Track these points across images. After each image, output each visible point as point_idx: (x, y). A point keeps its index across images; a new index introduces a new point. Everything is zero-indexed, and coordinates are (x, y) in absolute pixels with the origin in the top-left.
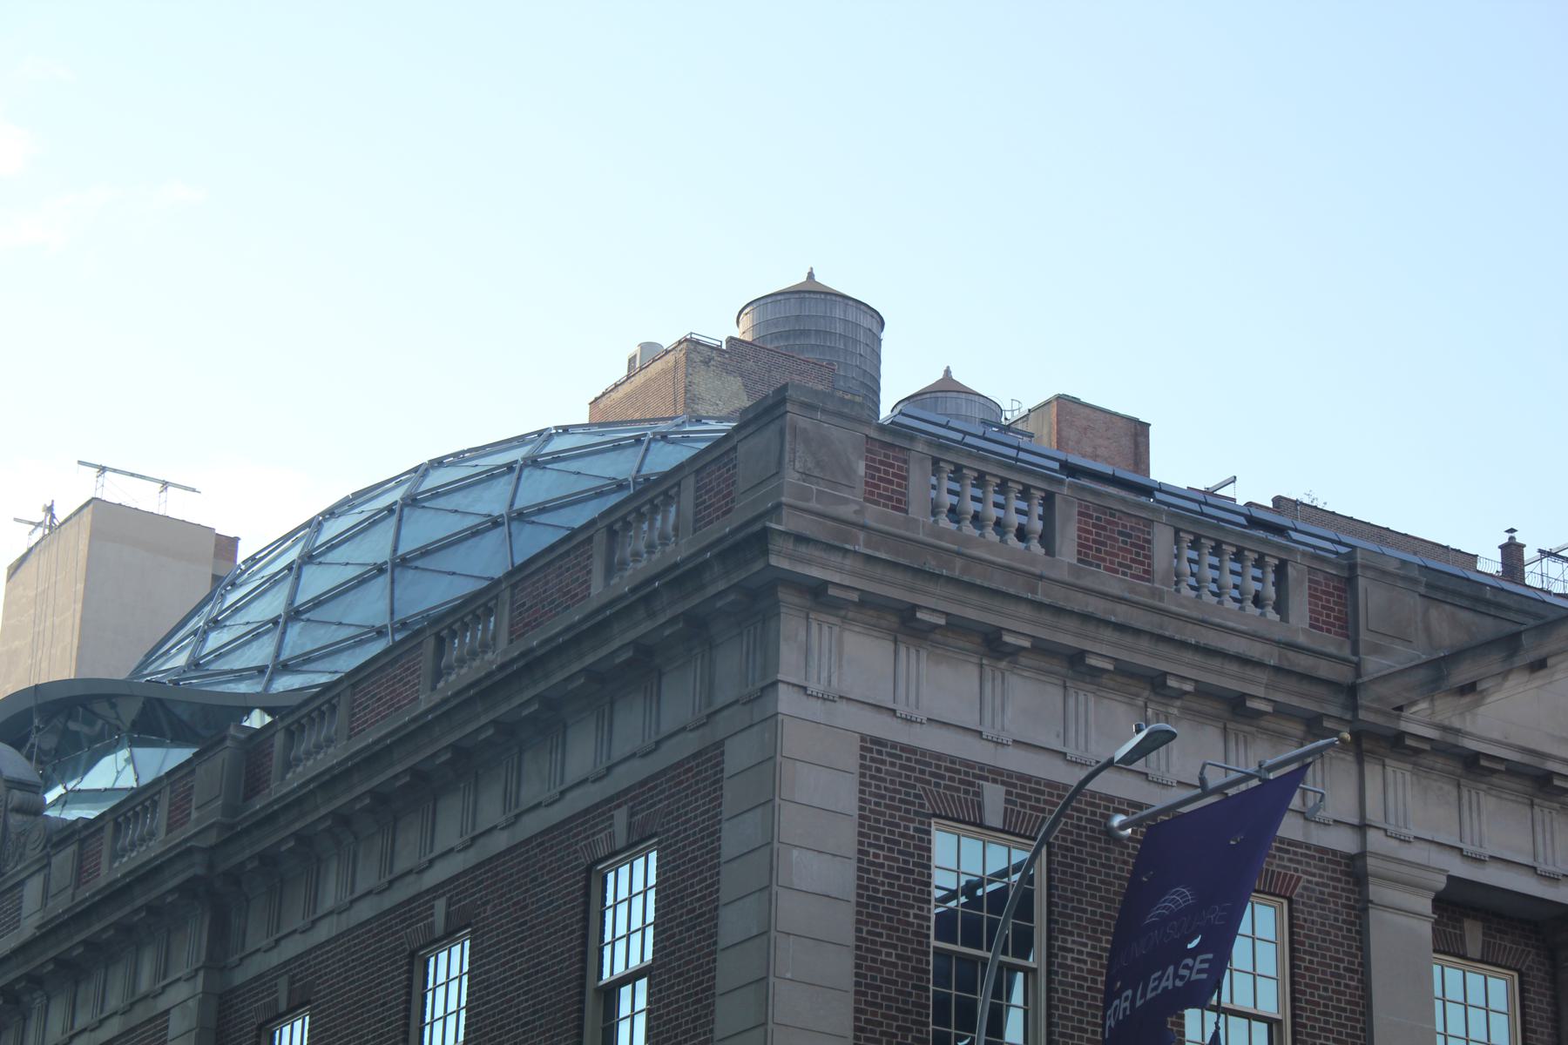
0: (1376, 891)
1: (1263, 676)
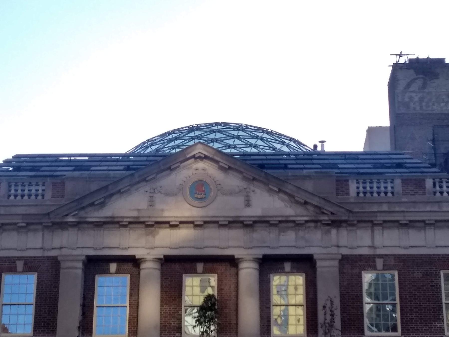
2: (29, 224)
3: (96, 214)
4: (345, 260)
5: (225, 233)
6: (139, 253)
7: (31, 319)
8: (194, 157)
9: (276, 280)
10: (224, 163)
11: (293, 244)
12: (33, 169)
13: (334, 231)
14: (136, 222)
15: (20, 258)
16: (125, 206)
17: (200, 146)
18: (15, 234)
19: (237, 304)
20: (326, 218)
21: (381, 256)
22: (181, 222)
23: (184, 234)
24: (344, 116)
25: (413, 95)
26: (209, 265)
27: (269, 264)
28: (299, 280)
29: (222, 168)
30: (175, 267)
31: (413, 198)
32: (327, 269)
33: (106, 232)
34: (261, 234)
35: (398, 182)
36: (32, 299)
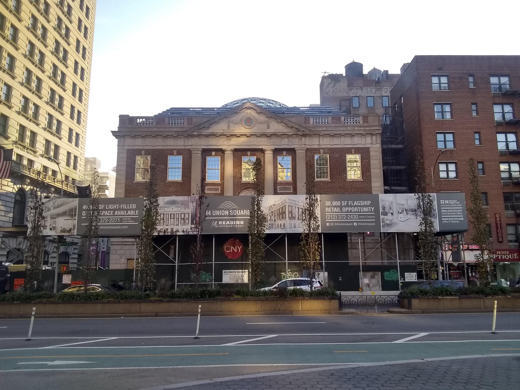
2: (178, 135)
3: (206, 132)
4: (307, 150)
5: (259, 139)
6: (224, 148)
7: (181, 174)
9: (279, 158)
10: (259, 110)
12: (179, 113)
13: (303, 139)
14: (222, 135)
15: (175, 149)
16: (218, 128)
17: (248, 103)
18: (172, 140)
21: (322, 148)
23: (243, 139)
24: (305, 95)
26: (252, 153)
27: (277, 152)
29: (257, 112)
30: (239, 153)
32: (301, 154)
33: (210, 139)
34: (274, 140)
35: (330, 118)
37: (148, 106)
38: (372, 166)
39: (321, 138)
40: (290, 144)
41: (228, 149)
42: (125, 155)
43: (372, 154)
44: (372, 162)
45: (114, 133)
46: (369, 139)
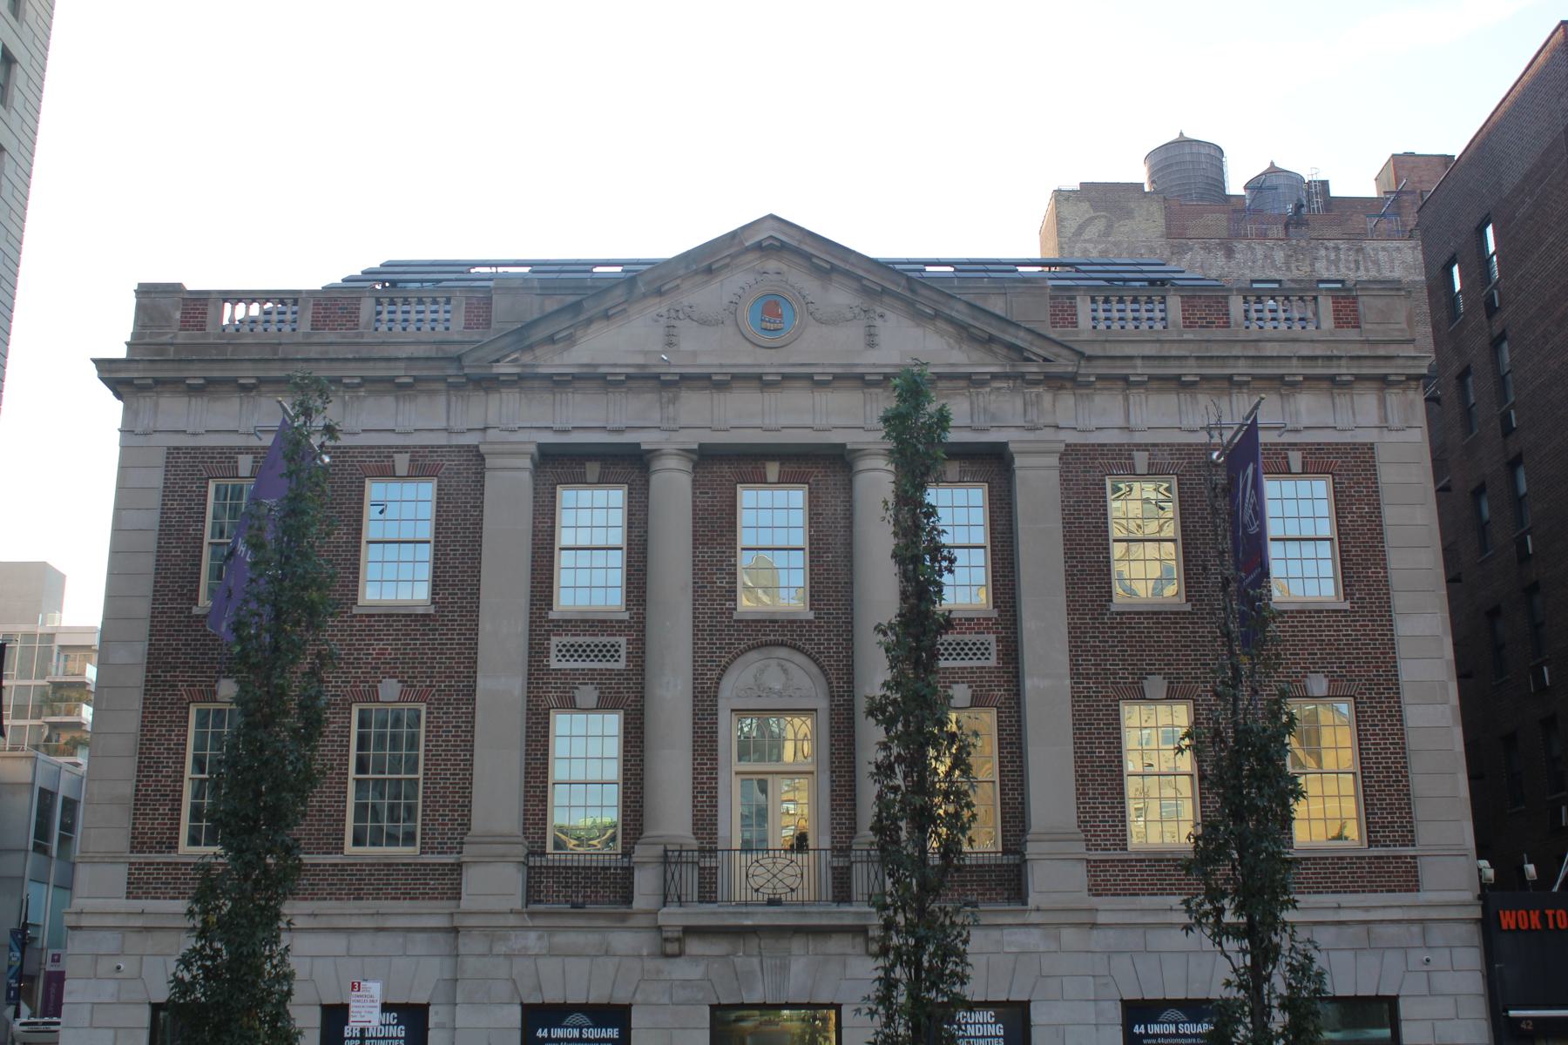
0: (489, 462)
1: (402, 365)
4: (1071, 455)
8: (759, 247)
11: (967, 422)
15: (402, 449)
18: (389, 401)
19: (849, 545)
20: (1035, 369)
21: (1140, 447)
22: (735, 377)
25: (1090, 246)
28: (977, 496)
31: (1206, 334)
33: (578, 397)
36: (426, 531)
37: (279, 242)
38: (1391, 536)
39: (1136, 397)
40: (981, 421)
41: (668, 448)
42: (157, 479)
43: (1387, 475)
44: (1390, 515)
45: (109, 371)
46: (1367, 404)
